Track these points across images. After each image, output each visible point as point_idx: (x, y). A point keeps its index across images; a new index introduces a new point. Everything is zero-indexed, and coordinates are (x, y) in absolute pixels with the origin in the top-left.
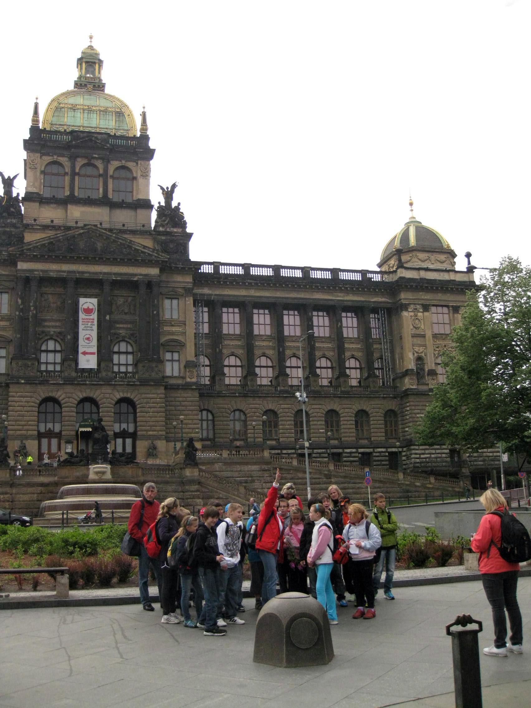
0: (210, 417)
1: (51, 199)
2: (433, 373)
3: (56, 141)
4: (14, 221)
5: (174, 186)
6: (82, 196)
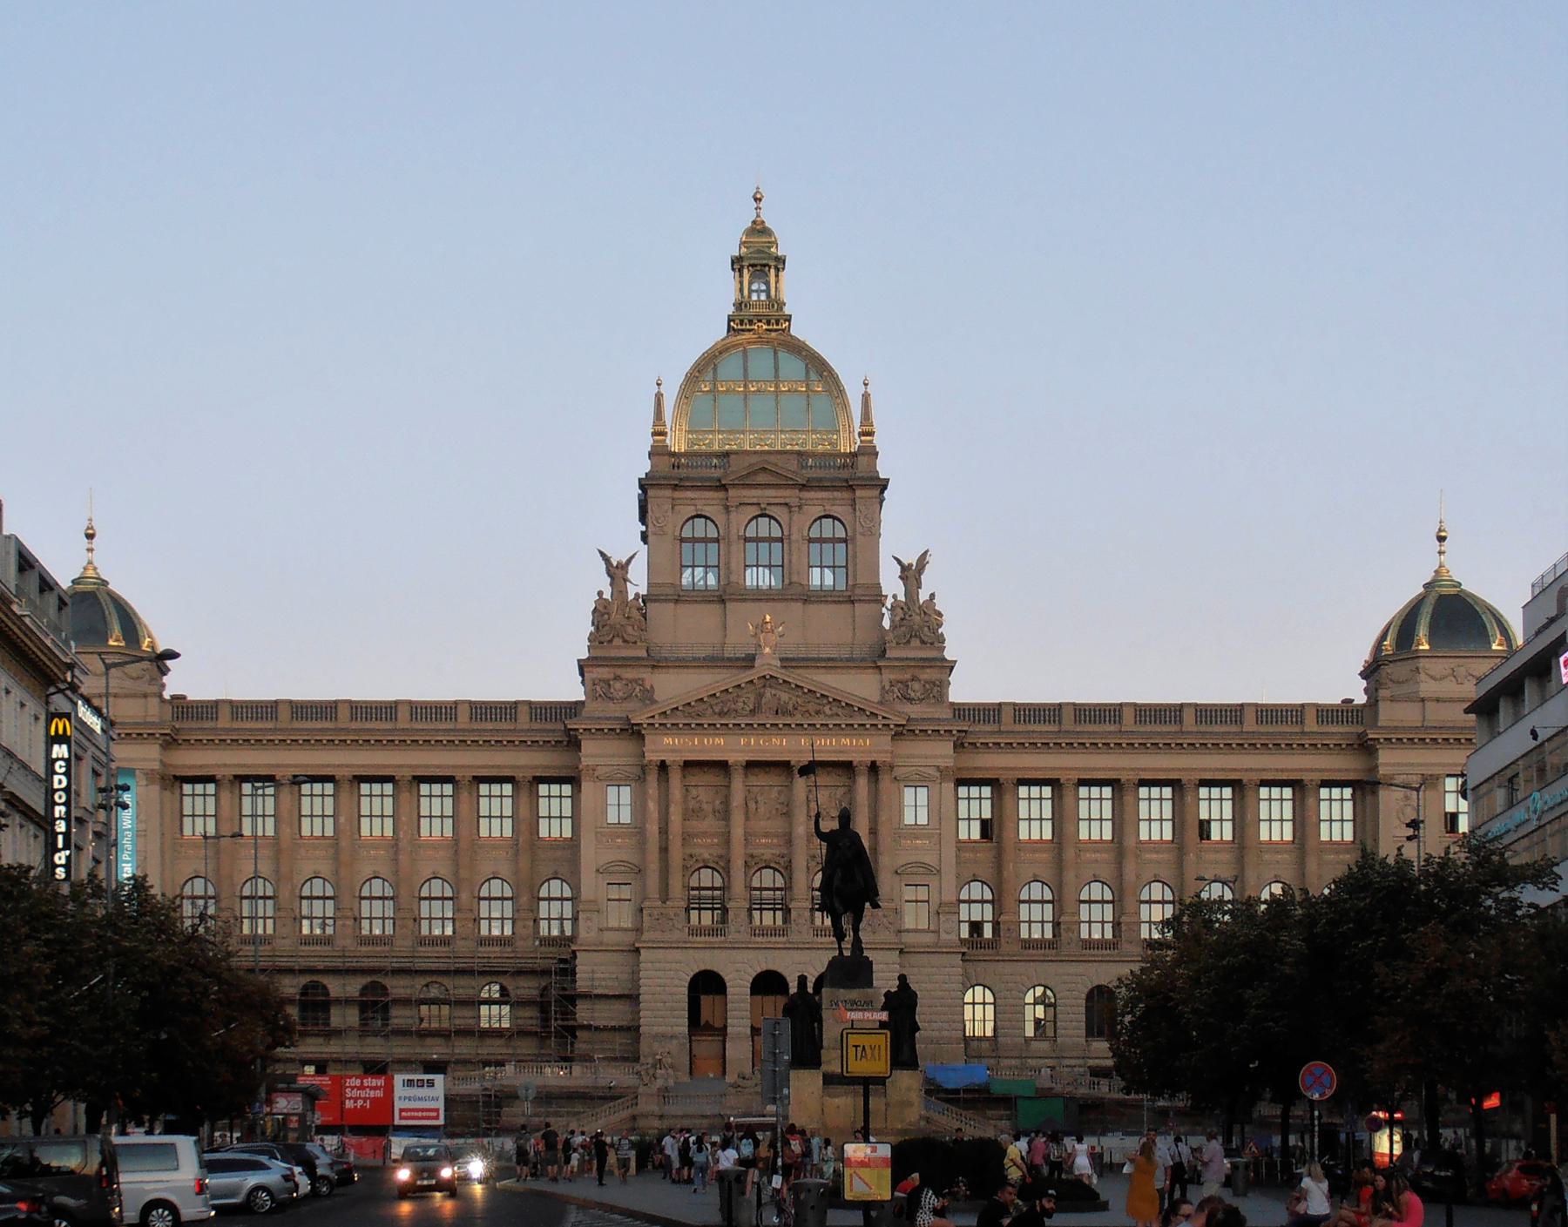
0: (989, 998)
5: (923, 561)
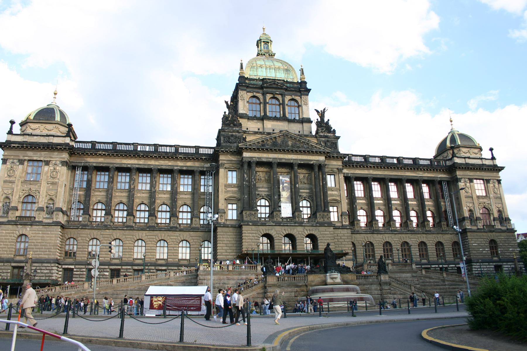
1: (254, 117)
3: (254, 84)
4: (237, 129)
6: (271, 116)
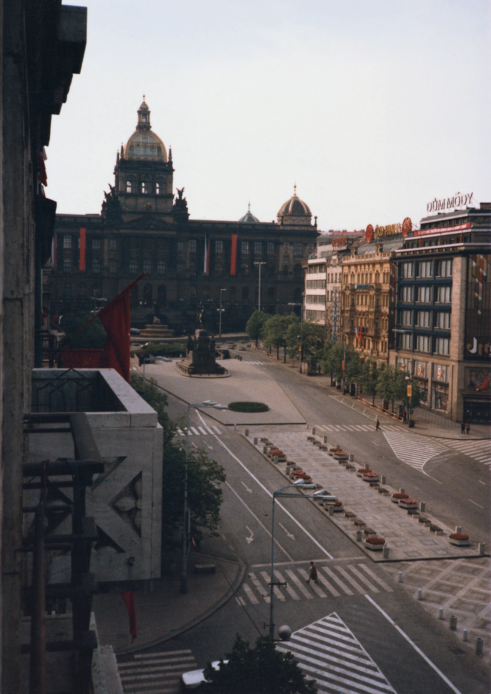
2: (291, 273)
